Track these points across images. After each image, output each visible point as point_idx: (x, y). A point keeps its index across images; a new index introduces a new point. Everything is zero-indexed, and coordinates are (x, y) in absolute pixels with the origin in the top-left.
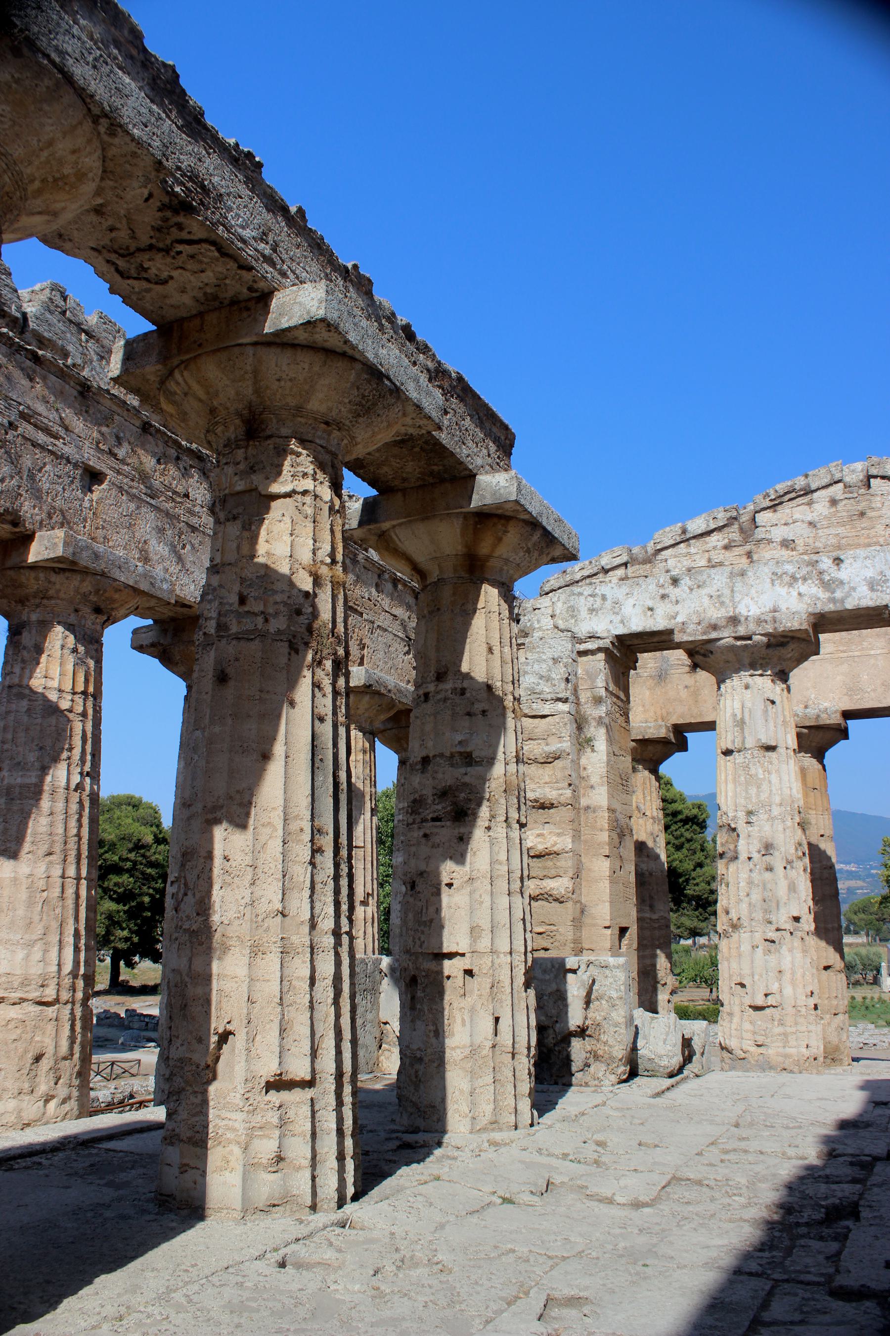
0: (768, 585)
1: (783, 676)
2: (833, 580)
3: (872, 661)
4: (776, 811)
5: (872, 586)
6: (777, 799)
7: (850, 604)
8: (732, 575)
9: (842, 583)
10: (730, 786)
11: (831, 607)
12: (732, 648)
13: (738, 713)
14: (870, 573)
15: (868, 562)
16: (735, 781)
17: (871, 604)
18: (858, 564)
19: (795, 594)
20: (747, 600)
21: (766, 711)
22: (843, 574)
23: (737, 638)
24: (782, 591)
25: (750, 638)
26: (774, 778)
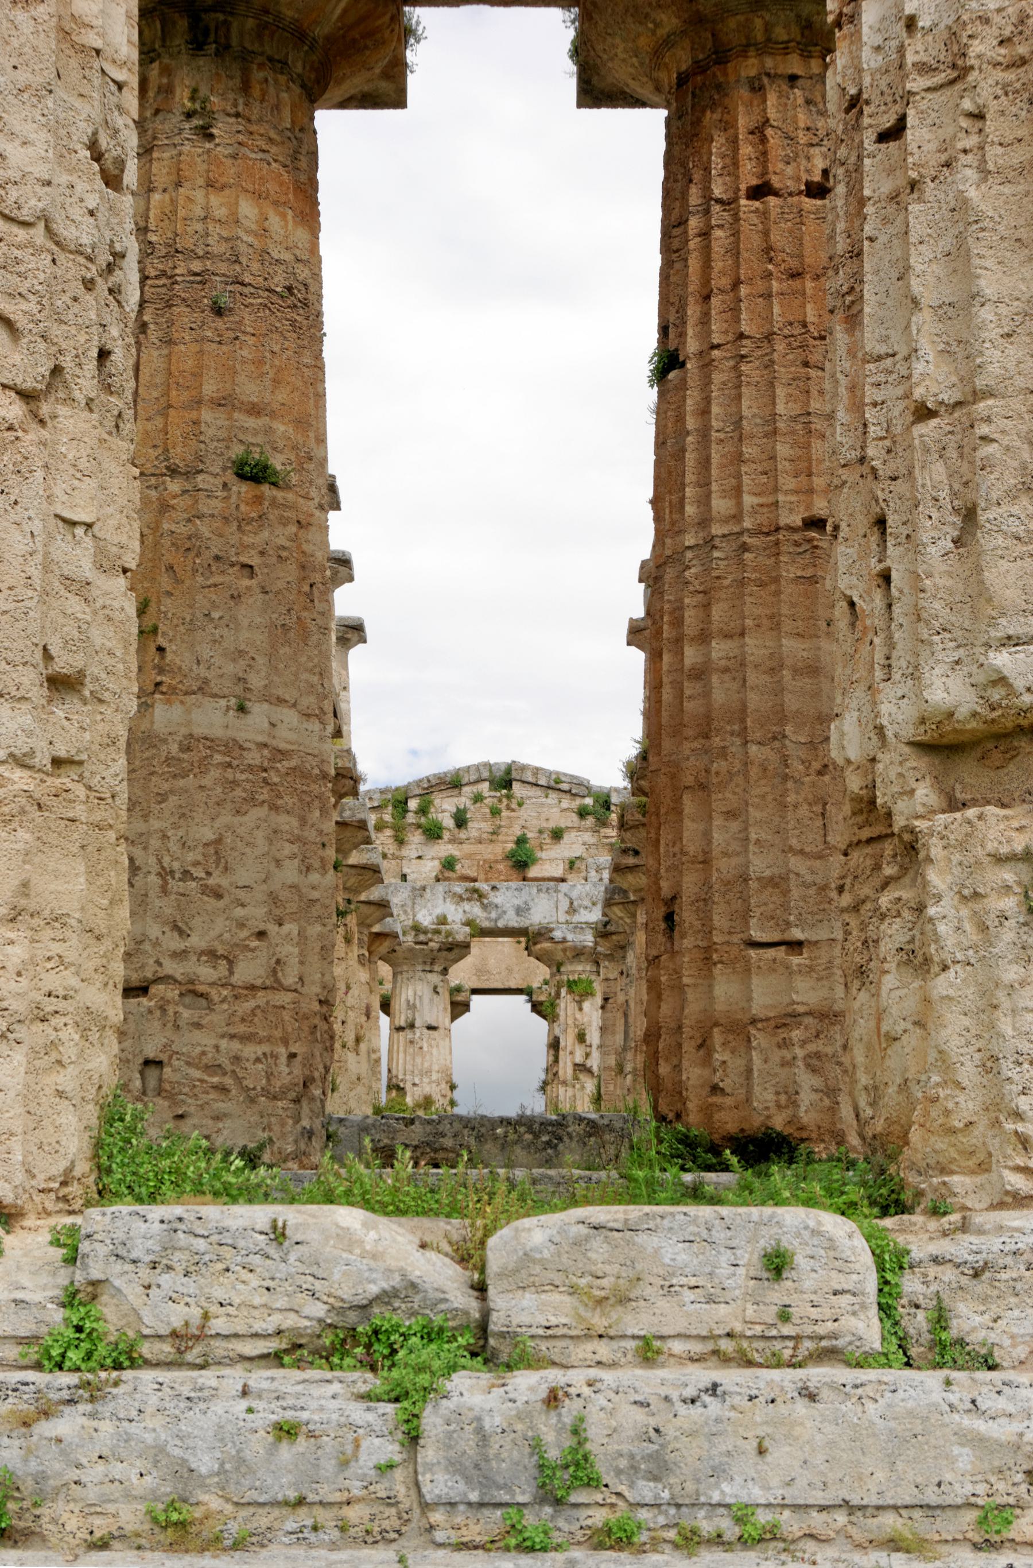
0: (441, 901)
1: (445, 971)
2: (490, 904)
3: (500, 947)
4: (434, 1077)
5: (519, 911)
6: (435, 1068)
7: (501, 924)
8: (414, 889)
9: (496, 906)
10: (401, 1055)
11: (486, 924)
12: (411, 950)
13: (411, 999)
14: (517, 902)
15: (516, 893)
16: (405, 1052)
17: (516, 925)
18: (509, 894)
19: (461, 911)
20: (424, 912)
21: (431, 1000)
22: (497, 898)
23: (416, 943)
24: (453, 907)
25: (426, 944)
26: (434, 1051)
